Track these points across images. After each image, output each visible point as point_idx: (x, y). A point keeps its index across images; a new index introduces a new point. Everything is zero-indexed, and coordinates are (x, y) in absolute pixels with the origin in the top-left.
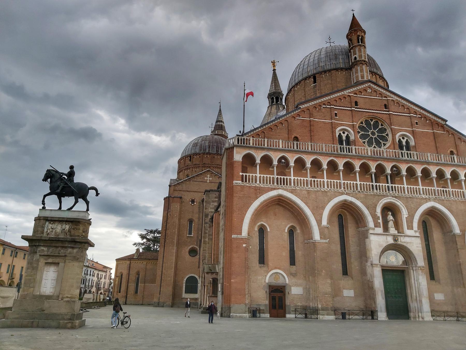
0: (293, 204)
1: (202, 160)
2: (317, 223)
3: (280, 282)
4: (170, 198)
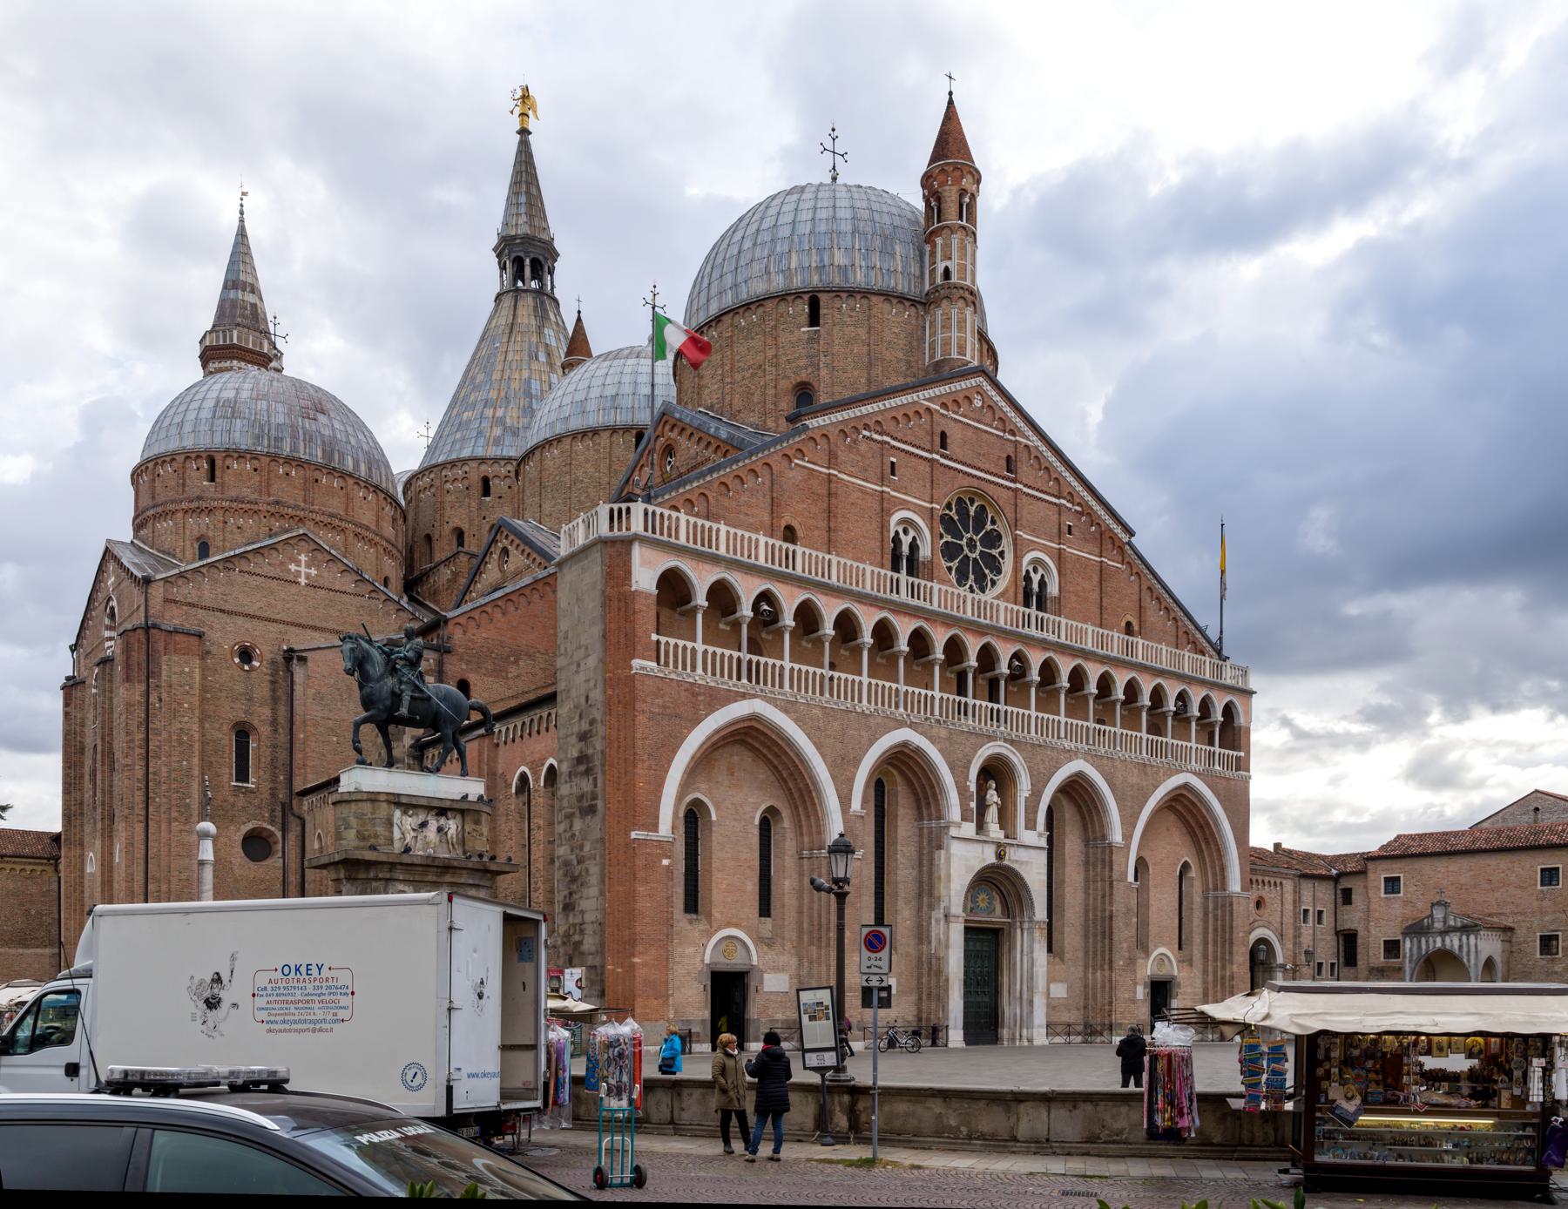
0: (783, 745)
1: (269, 485)
2: (841, 803)
3: (736, 962)
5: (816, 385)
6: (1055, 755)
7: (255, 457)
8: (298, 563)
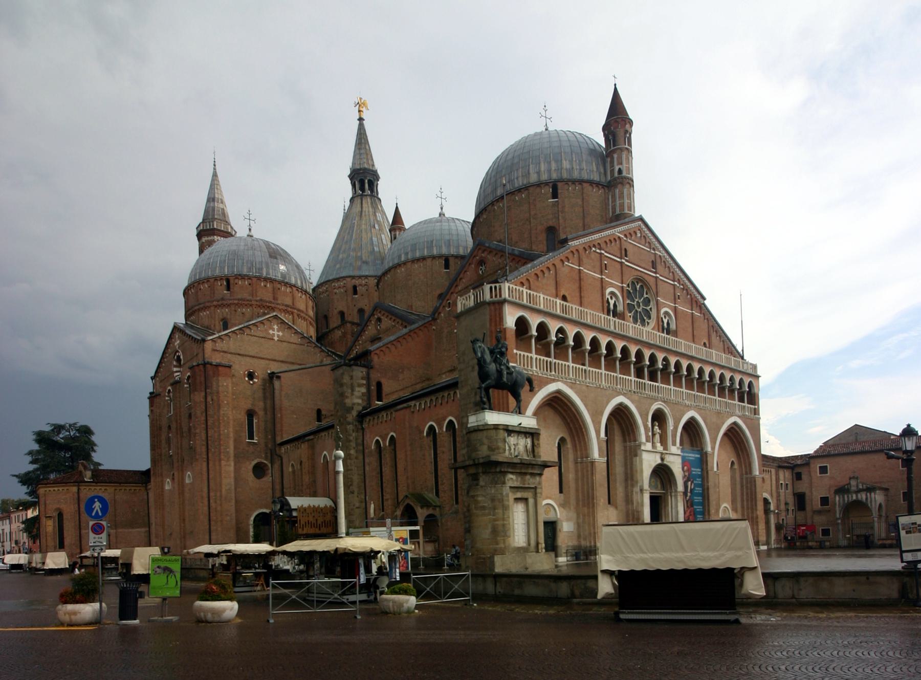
4: (208, 366)
5: (558, 228)
6: (682, 408)
7: (250, 278)
8: (273, 330)
